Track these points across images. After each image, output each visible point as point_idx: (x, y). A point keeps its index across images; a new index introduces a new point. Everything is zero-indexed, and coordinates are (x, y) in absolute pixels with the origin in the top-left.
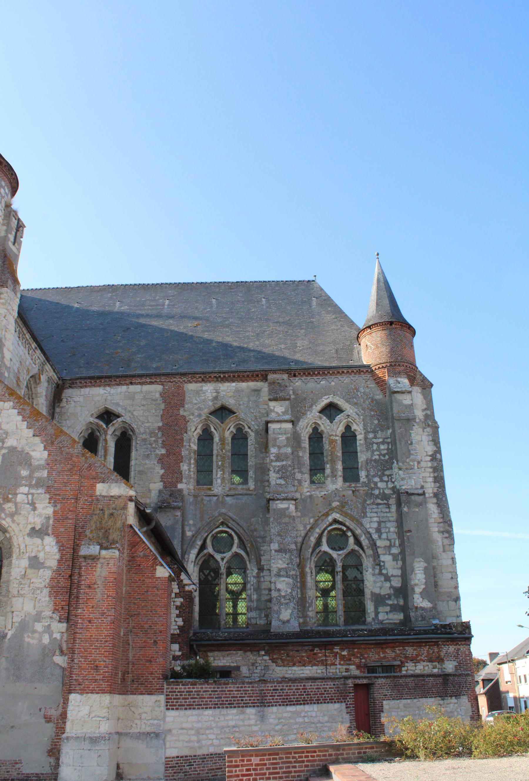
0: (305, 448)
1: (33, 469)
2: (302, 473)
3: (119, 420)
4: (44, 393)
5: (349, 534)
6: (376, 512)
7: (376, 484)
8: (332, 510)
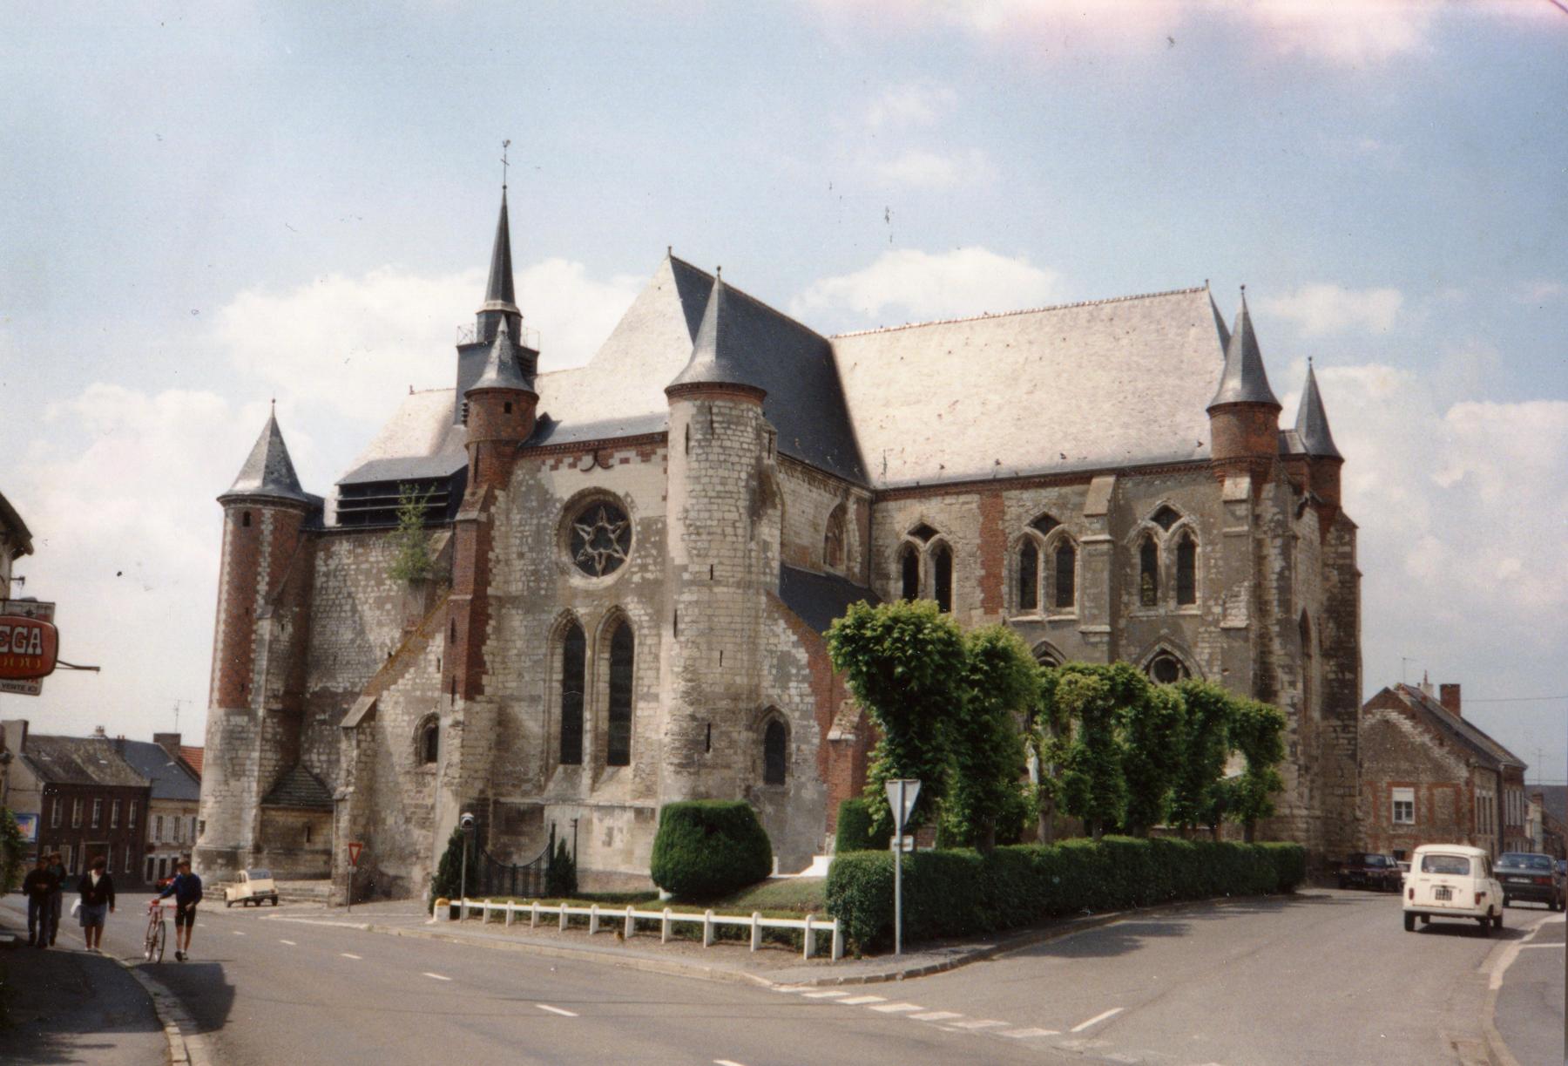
0: (1135, 564)
1: (800, 668)
2: (1129, 594)
3: (937, 537)
4: (854, 517)
5: (1179, 666)
6: (1208, 642)
7: (1209, 608)
8: (1159, 639)
